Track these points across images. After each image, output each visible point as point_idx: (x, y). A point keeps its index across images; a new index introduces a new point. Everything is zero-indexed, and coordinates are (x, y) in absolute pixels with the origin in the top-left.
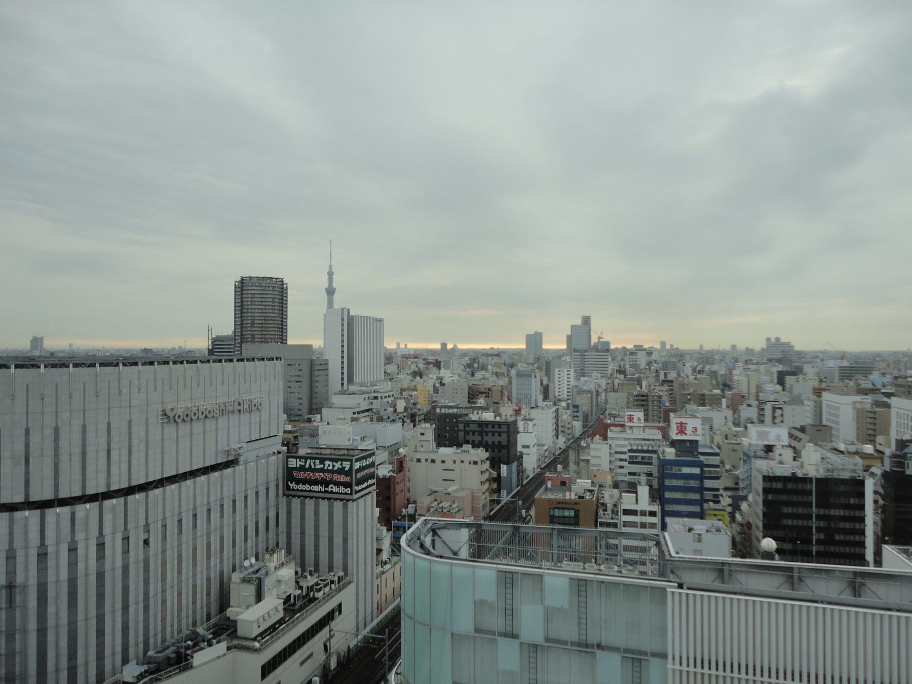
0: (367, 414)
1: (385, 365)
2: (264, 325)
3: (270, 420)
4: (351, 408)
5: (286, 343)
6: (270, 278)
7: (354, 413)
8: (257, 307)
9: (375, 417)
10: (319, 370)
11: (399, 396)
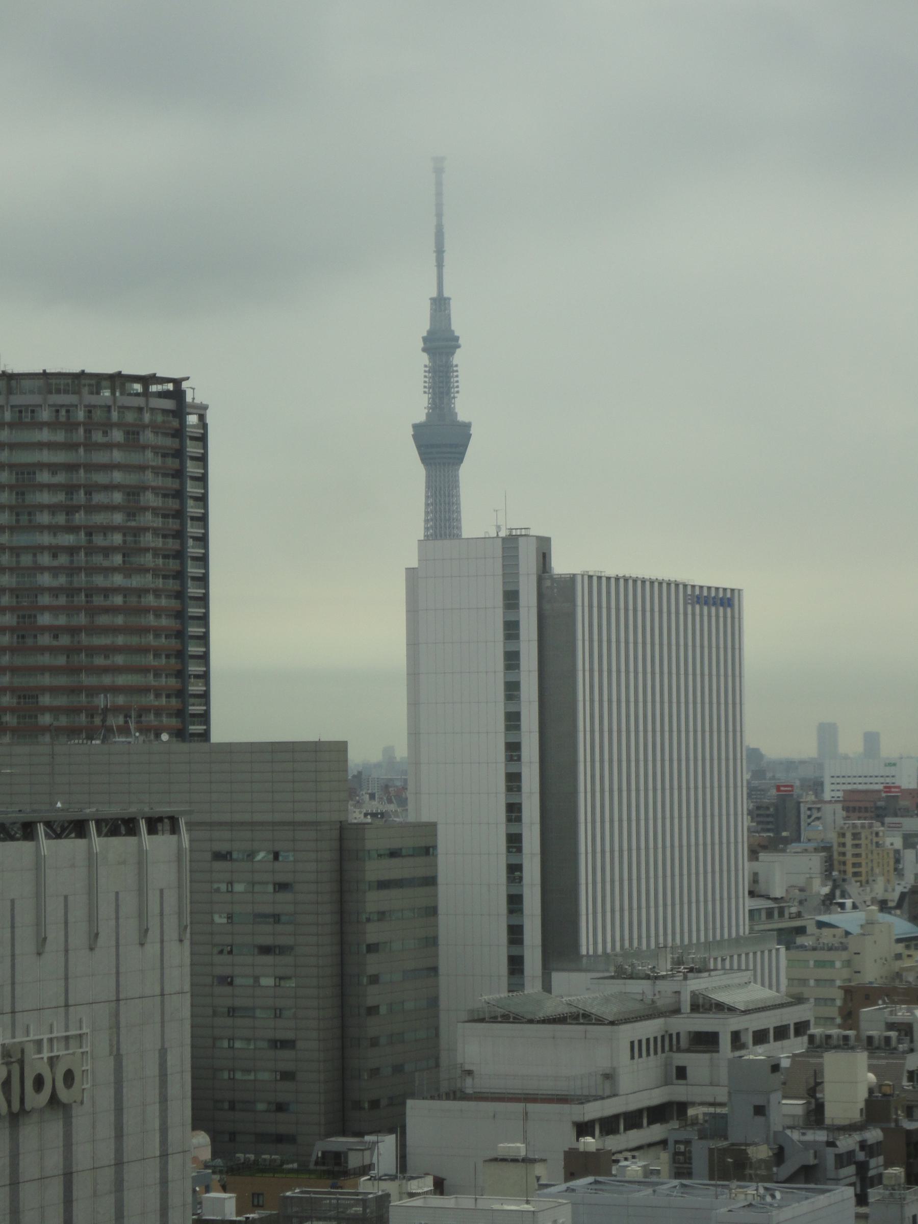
0: (656, 1132)
1: (754, 854)
2: (84, 639)
3: (119, 1164)
4: (562, 1099)
5: (205, 736)
6: (118, 380)
7: (583, 1129)
8: (46, 539)
9: (700, 1151)
10: (383, 885)
11: (834, 1031)
